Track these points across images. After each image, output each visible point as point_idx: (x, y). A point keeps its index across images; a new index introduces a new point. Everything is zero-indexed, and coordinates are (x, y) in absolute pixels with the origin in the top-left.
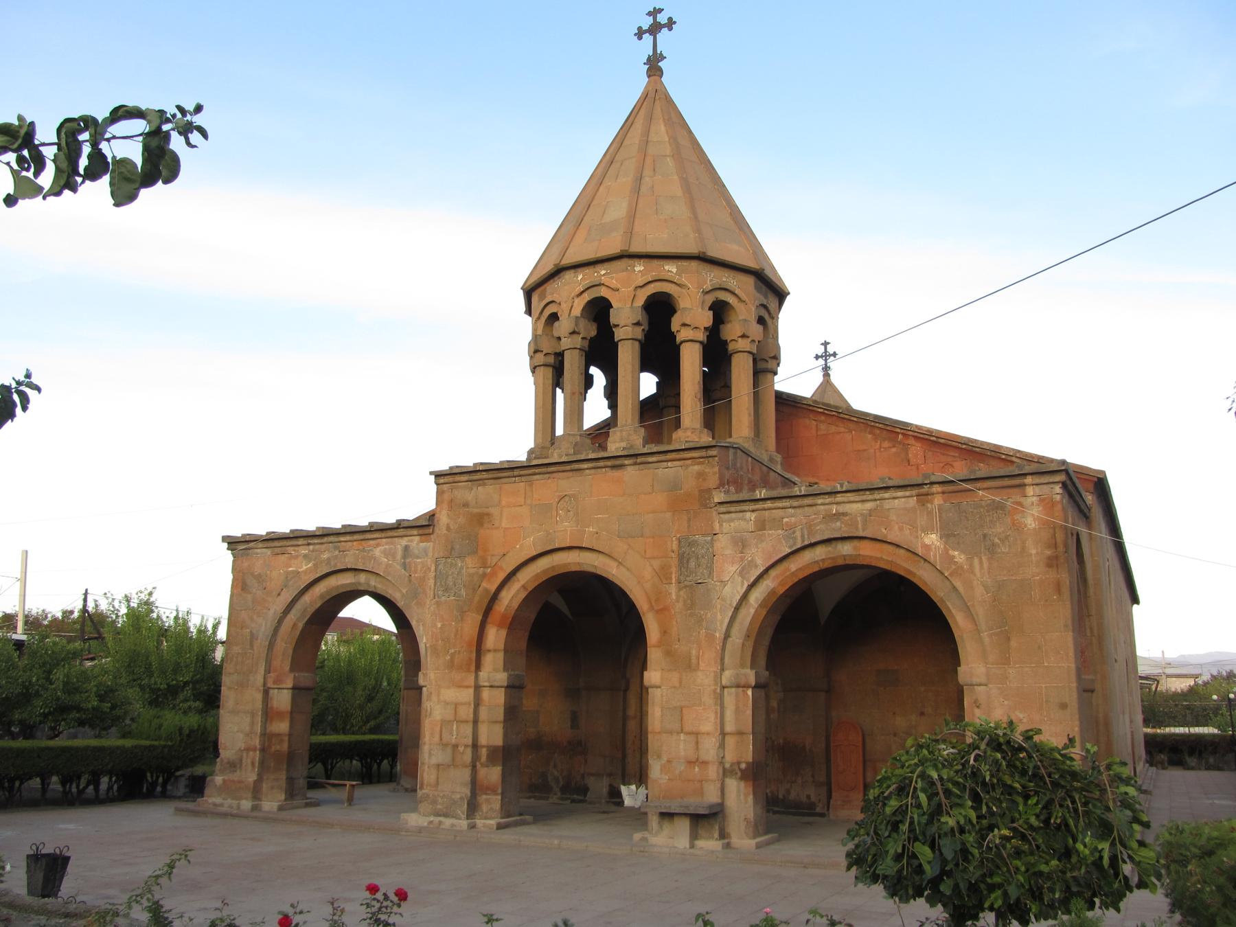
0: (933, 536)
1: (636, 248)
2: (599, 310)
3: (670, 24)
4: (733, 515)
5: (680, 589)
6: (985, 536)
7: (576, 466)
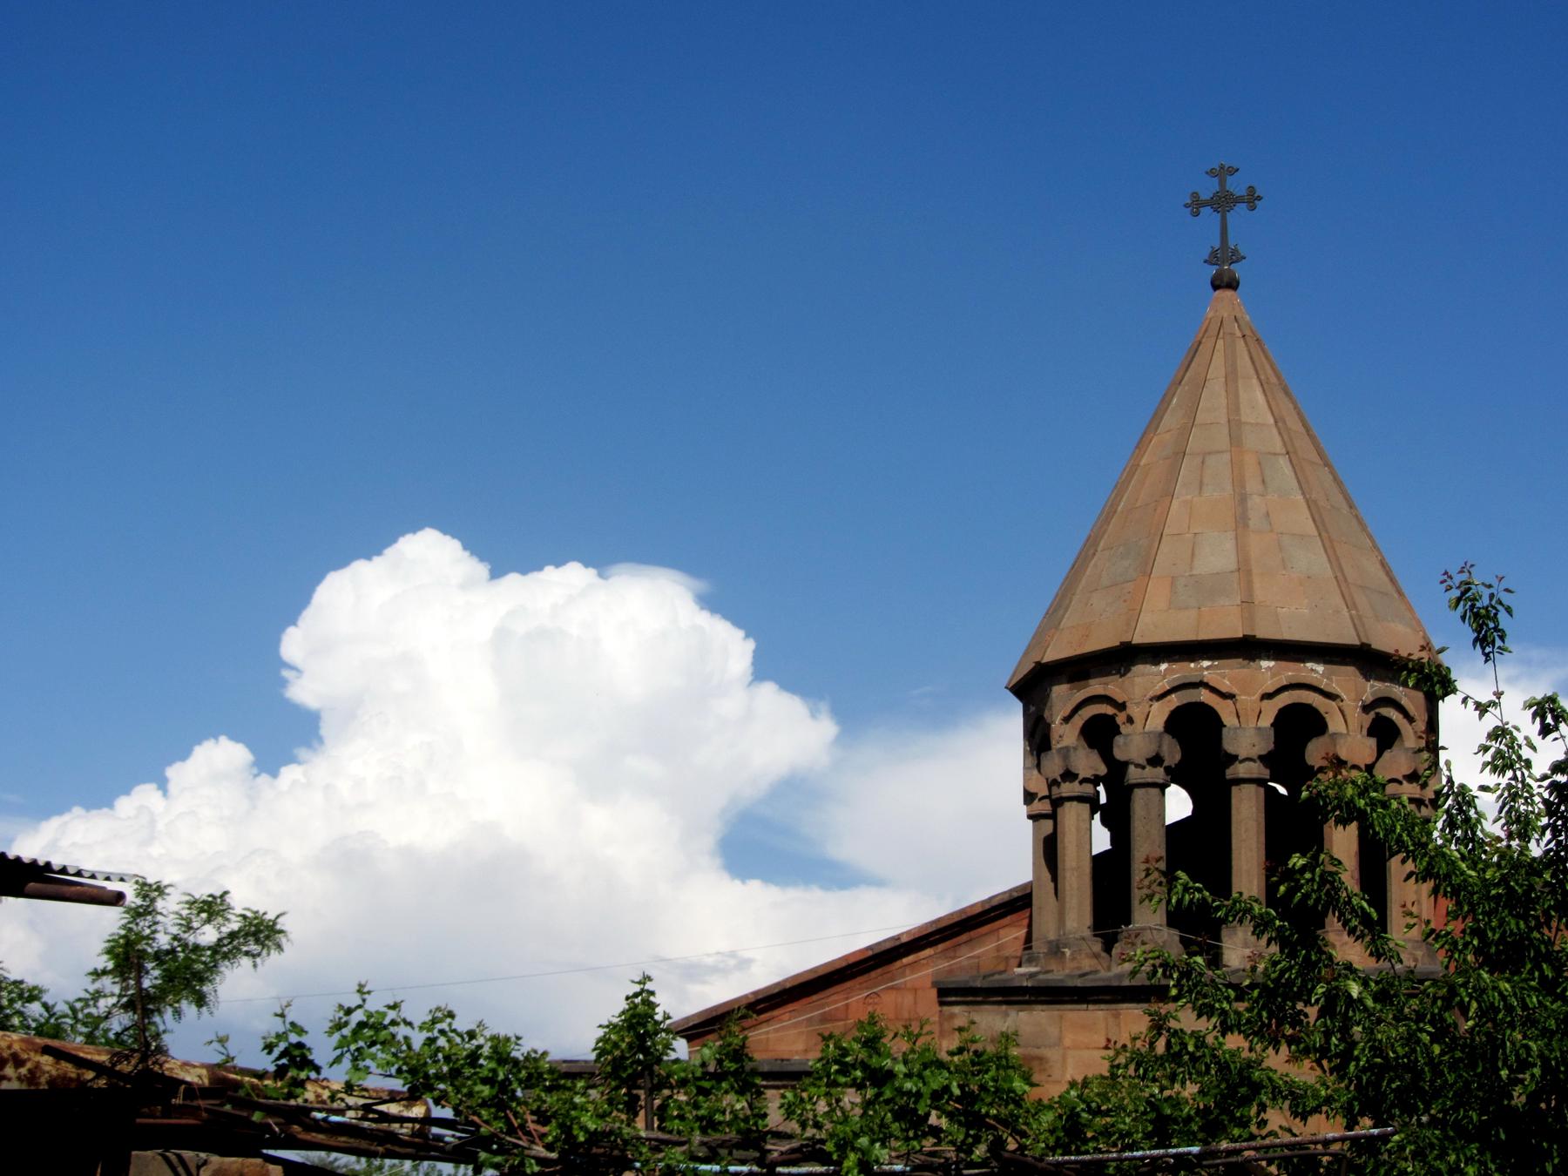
1: (1264, 631)
3: (1252, 199)
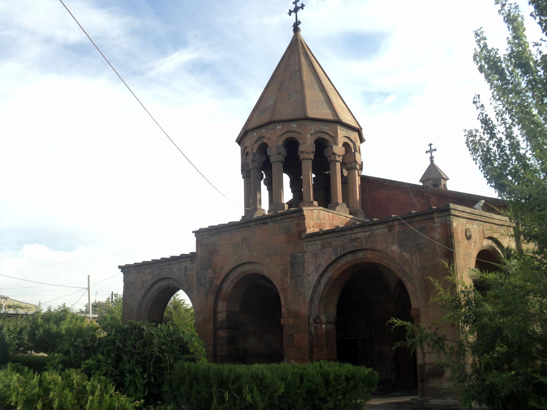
0: (395, 246)
1: (277, 118)
2: (263, 148)
3: (302, 6)
4: (312, 243)
5: (291, 279)
6: (417, 244)
7: (248, 224)
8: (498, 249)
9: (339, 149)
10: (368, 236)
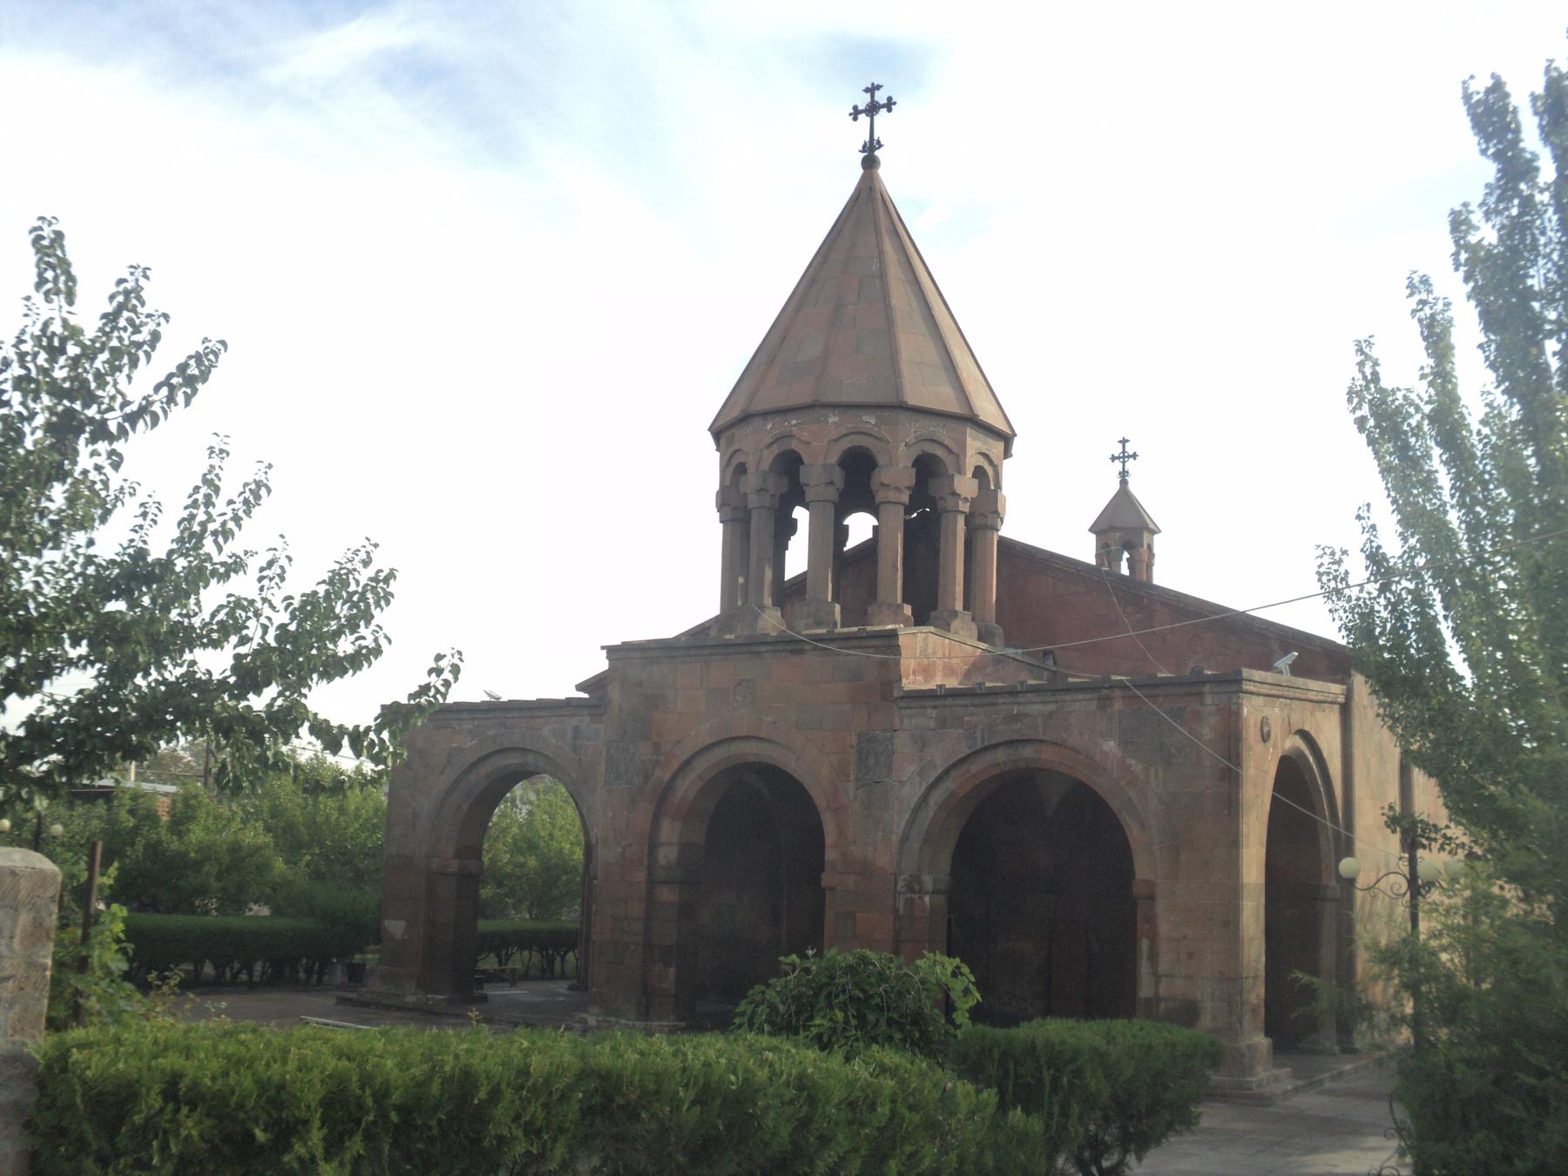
2: (790, 464)
3: (889, 105)
8: (1308, 753)
9: (966, 485)
10: (1051, 714)
